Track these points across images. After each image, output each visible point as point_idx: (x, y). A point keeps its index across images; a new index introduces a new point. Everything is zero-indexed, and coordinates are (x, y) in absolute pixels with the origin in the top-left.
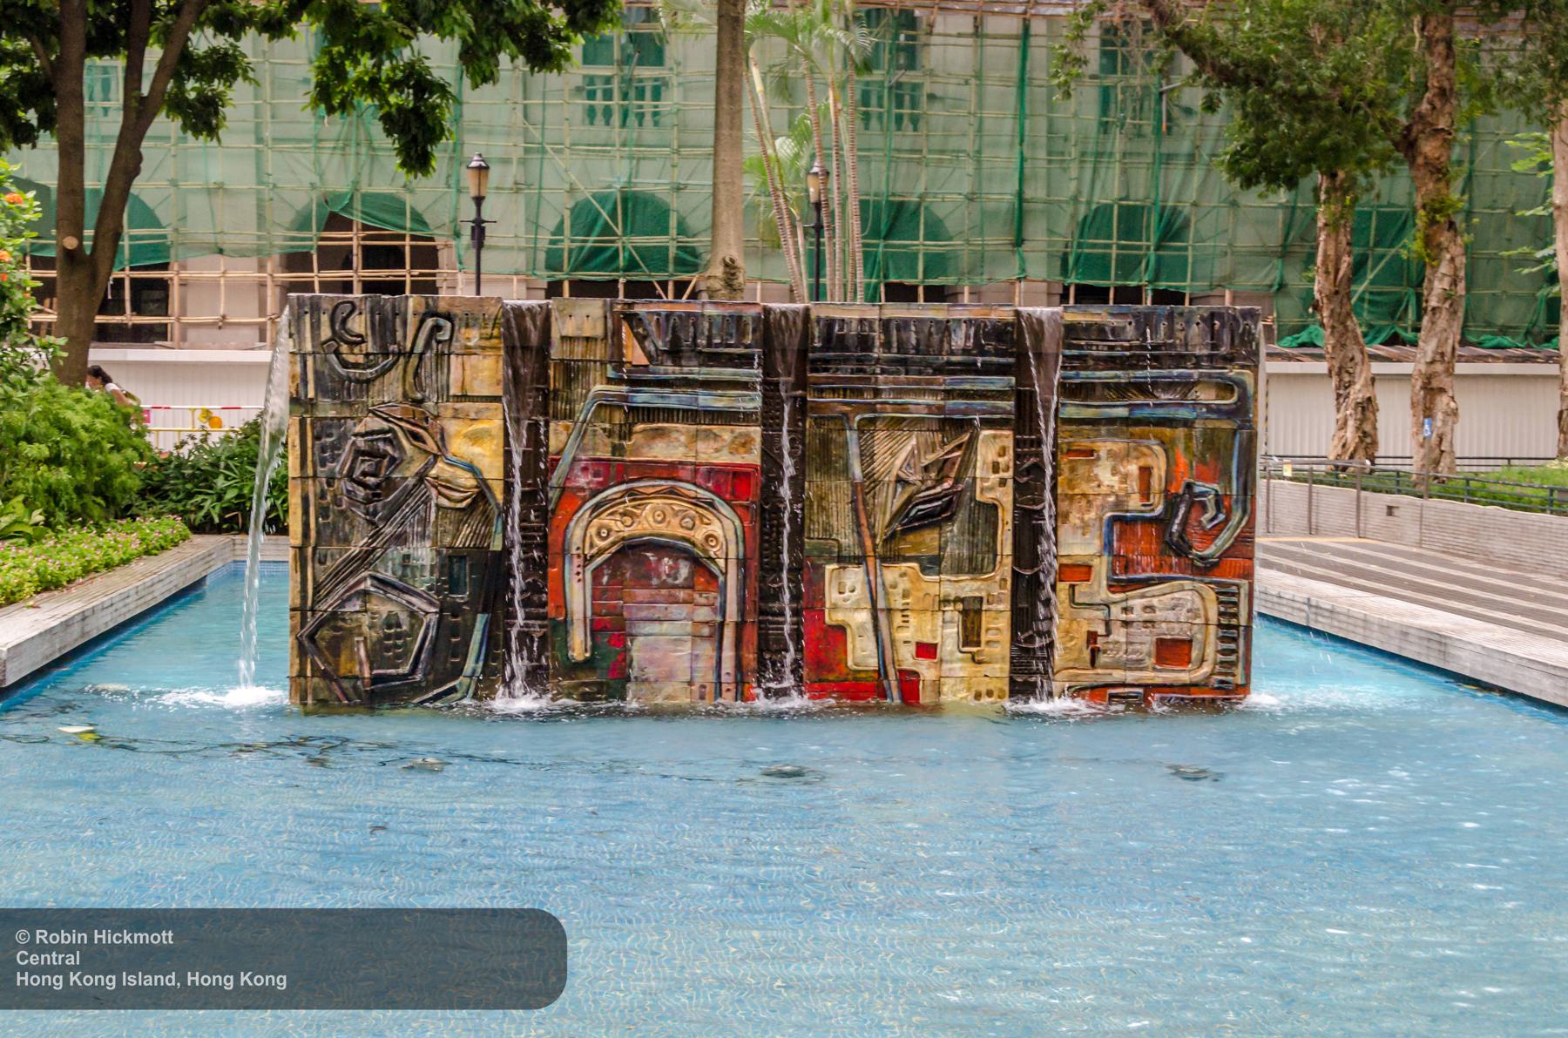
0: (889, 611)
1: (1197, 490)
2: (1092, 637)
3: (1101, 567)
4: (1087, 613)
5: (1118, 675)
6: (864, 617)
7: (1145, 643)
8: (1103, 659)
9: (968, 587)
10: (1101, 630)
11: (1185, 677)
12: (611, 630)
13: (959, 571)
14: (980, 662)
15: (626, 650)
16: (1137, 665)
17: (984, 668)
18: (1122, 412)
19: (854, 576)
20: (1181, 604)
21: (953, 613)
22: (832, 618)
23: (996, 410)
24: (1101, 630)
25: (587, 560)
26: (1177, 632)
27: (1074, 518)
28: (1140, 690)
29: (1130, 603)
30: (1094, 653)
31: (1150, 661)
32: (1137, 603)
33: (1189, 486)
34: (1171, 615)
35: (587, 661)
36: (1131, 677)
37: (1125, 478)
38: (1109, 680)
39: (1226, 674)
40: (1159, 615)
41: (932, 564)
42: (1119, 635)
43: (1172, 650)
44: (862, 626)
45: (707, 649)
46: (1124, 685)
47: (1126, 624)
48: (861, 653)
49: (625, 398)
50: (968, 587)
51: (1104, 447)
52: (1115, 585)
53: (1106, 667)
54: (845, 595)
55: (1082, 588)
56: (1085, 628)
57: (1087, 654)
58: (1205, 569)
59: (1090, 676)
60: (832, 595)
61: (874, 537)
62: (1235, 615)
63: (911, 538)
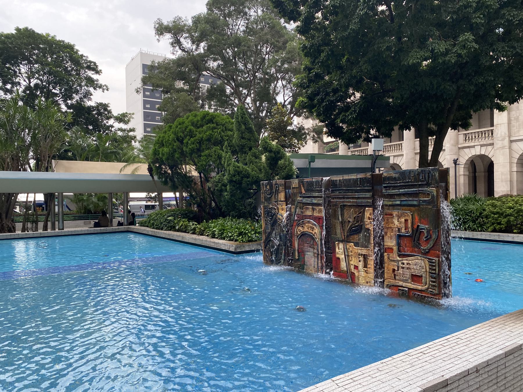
0: (348, 256)
1: (420, 227)
2: (394, 270)
3: (395, 248)
4: (393, 263)
5: (401, 283)
6: (343, 256)
7: (408, 274)
8: (397, 278)
9: (364, 251)
10: (396, 269)
11: (420, 288)
12: (302, 253)
13: (363, 247)
14: (367, 273)
15: (304, 258)
16: (405, 281)
17: (368, 275)
18: (398, 203)
19: (341, 246)
20: (418, 264)
21: (362, 259)
22: (337, 256)
23: (368, 202)
24: (396, 269)
25: (298, 236)
26: (417, 273)
27: (388, 235)
28: (407, 289)
29: (403, 261)
30: (395, 275)
31: (410, 281)
32: (405, 262)
33: (418, 226)
34: (415, 267)
35: (298, 259)
36: (404, 284)
37: (401, 223)
38: (398, 284)
39: (434, 289)
40: (411, 266)
41: (356, 245)
42: (401, 271)
43: (416, 278)
44: (342, 258)
45: (316, 260)
46: (402, 287)
47: (403, 268)
48: (343, 265)
49: (302, 201)
50: (364, 251)
51: (395, 213)
52: (399, 256)
53: (398, 280)
54: (340, 250)
55: (391, 255)
56: (392, 268)
57: (393, 275)
58: (425, 253)
59: (393, 282)
60: (337, 250)
61: (344, 236)
62: (435, 270)
63: (352, 236)
